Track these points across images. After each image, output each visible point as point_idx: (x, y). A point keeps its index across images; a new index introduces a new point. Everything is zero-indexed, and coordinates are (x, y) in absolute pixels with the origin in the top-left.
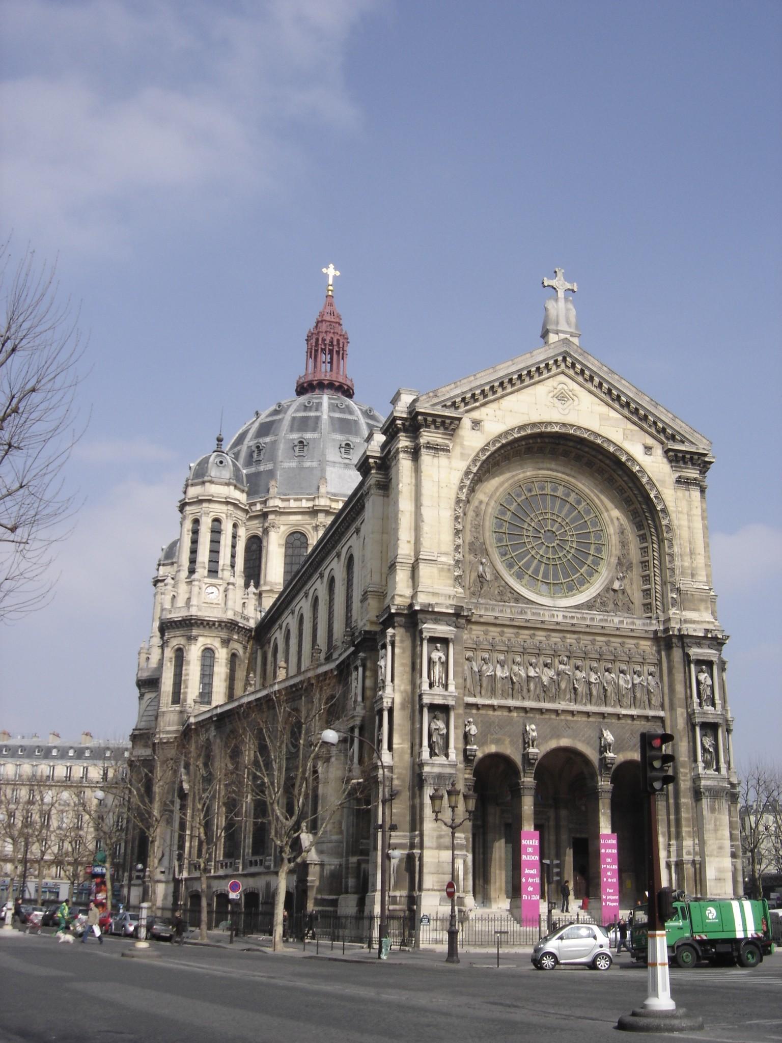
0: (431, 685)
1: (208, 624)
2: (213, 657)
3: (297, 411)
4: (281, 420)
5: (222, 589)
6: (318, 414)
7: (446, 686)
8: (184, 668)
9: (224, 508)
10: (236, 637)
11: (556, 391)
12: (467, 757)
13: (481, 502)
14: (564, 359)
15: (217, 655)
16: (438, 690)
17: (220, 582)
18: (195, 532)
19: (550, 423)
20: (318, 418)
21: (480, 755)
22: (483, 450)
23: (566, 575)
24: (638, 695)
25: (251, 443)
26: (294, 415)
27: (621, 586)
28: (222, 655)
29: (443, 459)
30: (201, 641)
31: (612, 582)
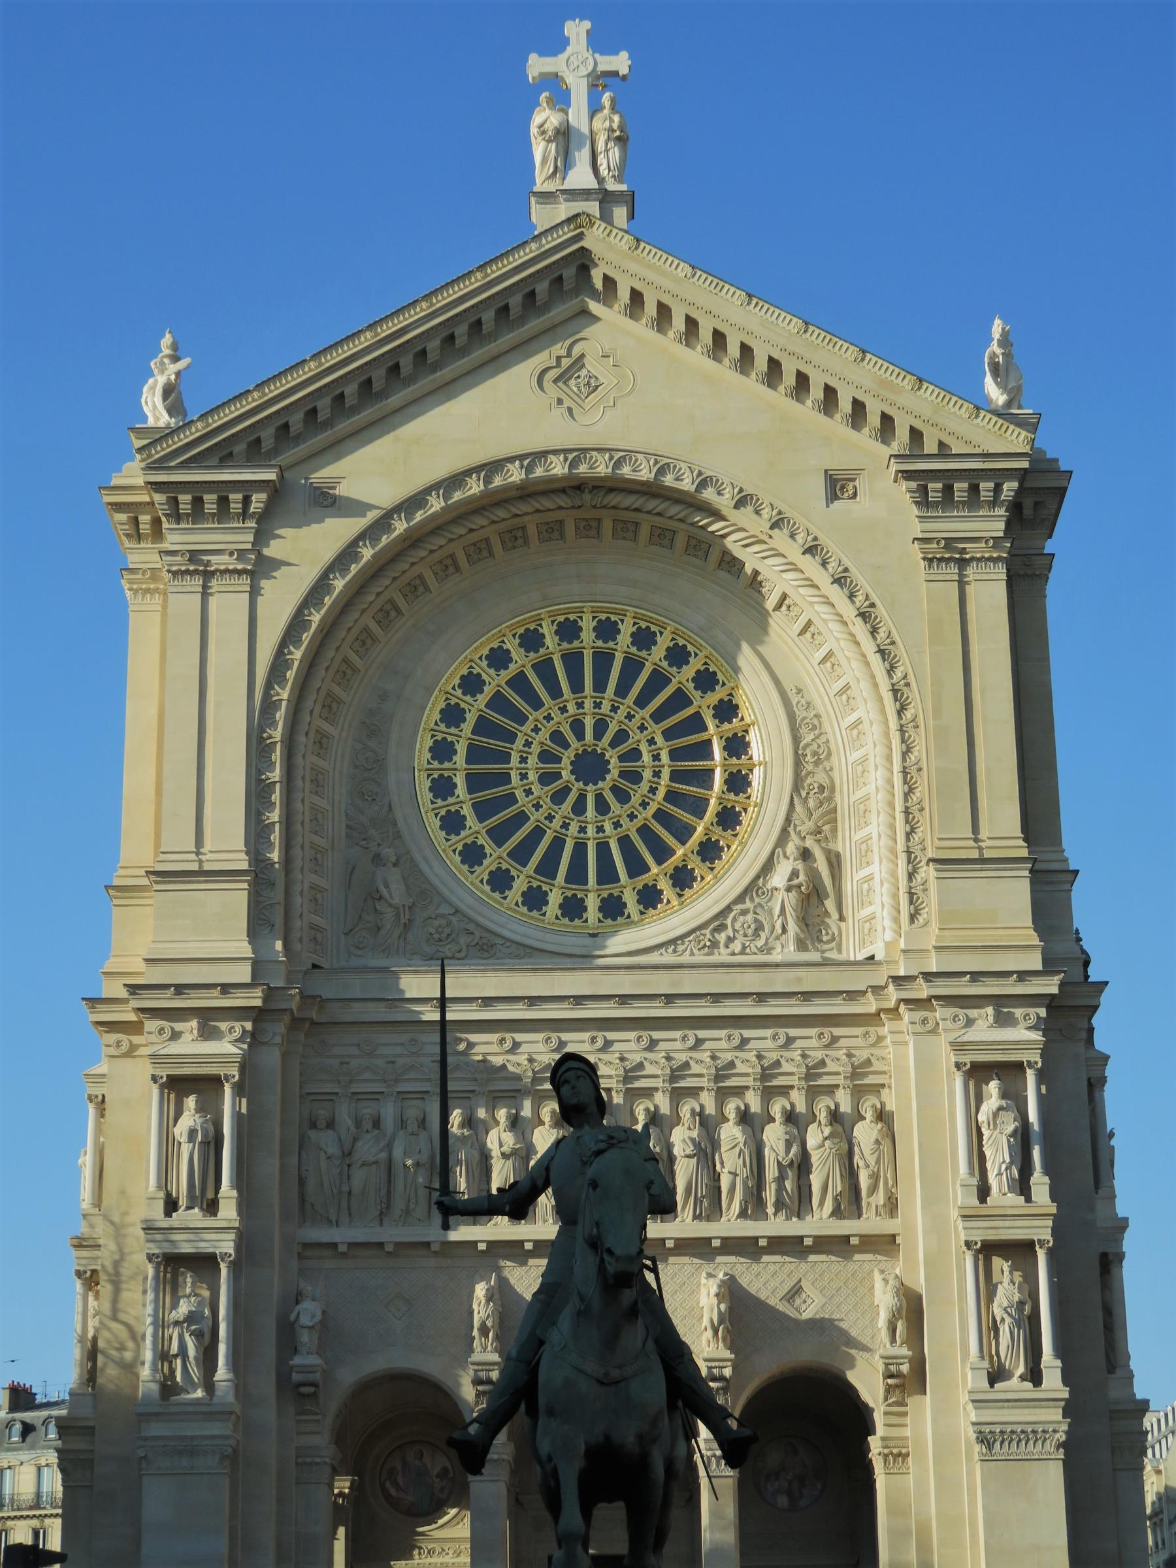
0: (171, 1206)
12: (298, 1393)
19: (542, 455)
21: (348, 1376)
22: (348, 554)
24: (816, 1180)
27: (794, 874)
31: (768, 867)
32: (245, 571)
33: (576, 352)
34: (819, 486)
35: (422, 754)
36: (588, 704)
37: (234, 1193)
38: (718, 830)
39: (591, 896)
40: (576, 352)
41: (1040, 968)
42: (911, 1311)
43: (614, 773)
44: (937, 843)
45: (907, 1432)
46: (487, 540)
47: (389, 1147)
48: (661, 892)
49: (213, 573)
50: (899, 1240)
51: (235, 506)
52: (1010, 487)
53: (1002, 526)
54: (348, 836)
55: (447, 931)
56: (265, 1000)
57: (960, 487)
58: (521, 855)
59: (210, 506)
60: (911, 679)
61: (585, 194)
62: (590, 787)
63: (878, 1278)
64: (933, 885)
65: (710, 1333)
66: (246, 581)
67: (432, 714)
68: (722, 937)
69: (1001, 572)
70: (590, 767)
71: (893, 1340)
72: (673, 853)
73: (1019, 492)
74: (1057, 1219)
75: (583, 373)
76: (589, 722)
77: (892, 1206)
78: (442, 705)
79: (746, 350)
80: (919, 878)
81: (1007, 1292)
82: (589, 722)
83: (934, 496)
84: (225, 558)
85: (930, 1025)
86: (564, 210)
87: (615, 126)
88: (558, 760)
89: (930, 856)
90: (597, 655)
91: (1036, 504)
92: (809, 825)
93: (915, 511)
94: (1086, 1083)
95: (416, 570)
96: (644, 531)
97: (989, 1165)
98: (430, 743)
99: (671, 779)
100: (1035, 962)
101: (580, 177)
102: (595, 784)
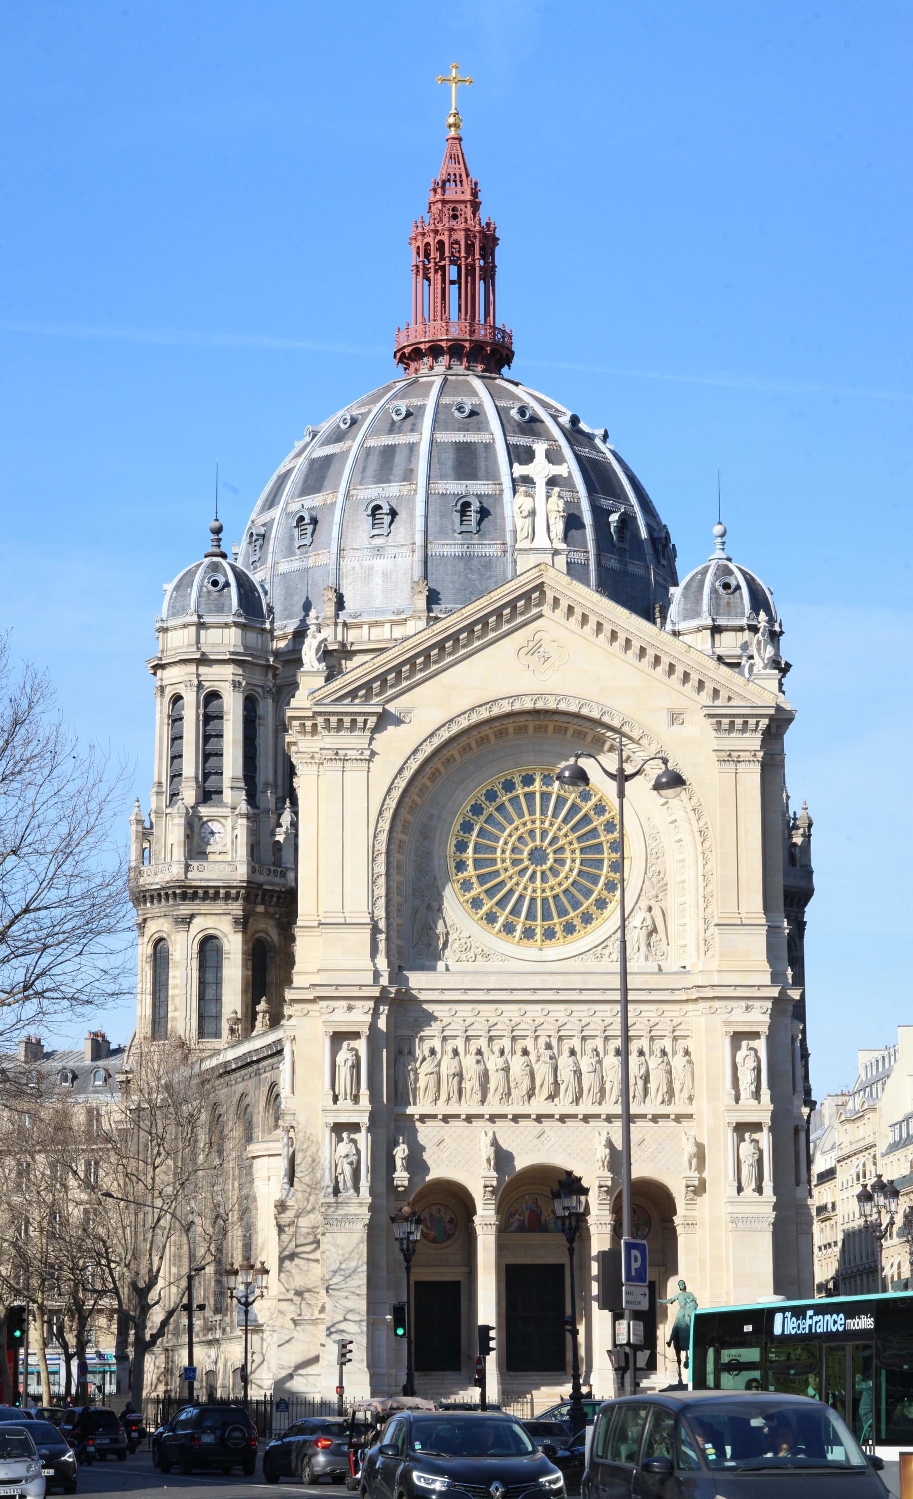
1: (206, 893)
2: (219, 951)
3: (374, 432)
4: (345, 454)
5: (229, 823)
6: (412, 438)
7: (356, 1099)
8: (170, 974)
9: (229, 671)
10: (260, 909)
11: (531, 644)
13: (431, 817)
14: (543, 593)
15: (226, 947)
16: (345, 1103)
17: (227, 811)
18: (176, 720)
20: (412, 448)
23: (562, 912)
25: (295, 507)
26: (370, 443)
28: (233, 946)
29: (355, 776)
30: (198, 924)
32: (365, 760)
33: (537, 638)
34: (665, 718)
35: (451, 848)
36: (538, 822)
37: (368, 1092)
38: (605, 892)
39: (539, 927)
40: (537, 638)
41: (769, 983)
42: (700, 1155)
43: (550, 862)
44: (720, 915)
45: (696, 1213)
46: (487, 736)
47: (439, 1065)
48: (575, 926)
49: (347, 760)
50: (694, 1117)
51: (360, 724)
52: (764, 723)
53: (759, 743)
54: (413, 894)
55: (465, 946)
56: (381, 993)
57: (739, 722)
58: (501, 903)
59: (347, 724)
60: (709, 825)
61: (544, 550)
62: (539, 868)
63: (684, 1137)
64: (717, 937)
65: (600, 1163)
66: (365, 764)
67: (456, 826)
68: (606, 951)
69: (758, 767)
70: (537, 856)
71: (690, 1169)
72: (582, 904)
73: (769, 727)
74: (773, 1113)
75: (541, 649)
76: (538, 832)
77: (691, 1098)
78: (461, 821)
79: (628, 641)
80: (709, 932)
81: (746, 1148)
82: (538, 832)
83: (724, 727)
84: (355, 752)
85: (713, 1010)
86: (533, 559)
87: (561, 509)
88: (521, 852)
89: (716, 922)
90: (543, 794)
91: (778, 726)
92: (654, 893)
93: (714, 734)
94: (790, 1038)
95: (451, 753)
96: (570, 731)
97: (740, 1083)
98: (454, 842)
99: (581, 864)
100: (767, 980)
101: (541, 541)
102: (541, 866)
